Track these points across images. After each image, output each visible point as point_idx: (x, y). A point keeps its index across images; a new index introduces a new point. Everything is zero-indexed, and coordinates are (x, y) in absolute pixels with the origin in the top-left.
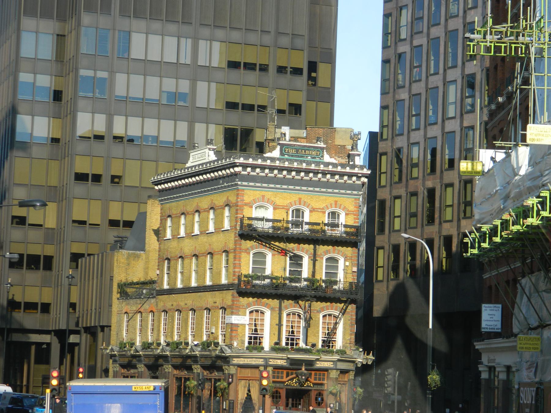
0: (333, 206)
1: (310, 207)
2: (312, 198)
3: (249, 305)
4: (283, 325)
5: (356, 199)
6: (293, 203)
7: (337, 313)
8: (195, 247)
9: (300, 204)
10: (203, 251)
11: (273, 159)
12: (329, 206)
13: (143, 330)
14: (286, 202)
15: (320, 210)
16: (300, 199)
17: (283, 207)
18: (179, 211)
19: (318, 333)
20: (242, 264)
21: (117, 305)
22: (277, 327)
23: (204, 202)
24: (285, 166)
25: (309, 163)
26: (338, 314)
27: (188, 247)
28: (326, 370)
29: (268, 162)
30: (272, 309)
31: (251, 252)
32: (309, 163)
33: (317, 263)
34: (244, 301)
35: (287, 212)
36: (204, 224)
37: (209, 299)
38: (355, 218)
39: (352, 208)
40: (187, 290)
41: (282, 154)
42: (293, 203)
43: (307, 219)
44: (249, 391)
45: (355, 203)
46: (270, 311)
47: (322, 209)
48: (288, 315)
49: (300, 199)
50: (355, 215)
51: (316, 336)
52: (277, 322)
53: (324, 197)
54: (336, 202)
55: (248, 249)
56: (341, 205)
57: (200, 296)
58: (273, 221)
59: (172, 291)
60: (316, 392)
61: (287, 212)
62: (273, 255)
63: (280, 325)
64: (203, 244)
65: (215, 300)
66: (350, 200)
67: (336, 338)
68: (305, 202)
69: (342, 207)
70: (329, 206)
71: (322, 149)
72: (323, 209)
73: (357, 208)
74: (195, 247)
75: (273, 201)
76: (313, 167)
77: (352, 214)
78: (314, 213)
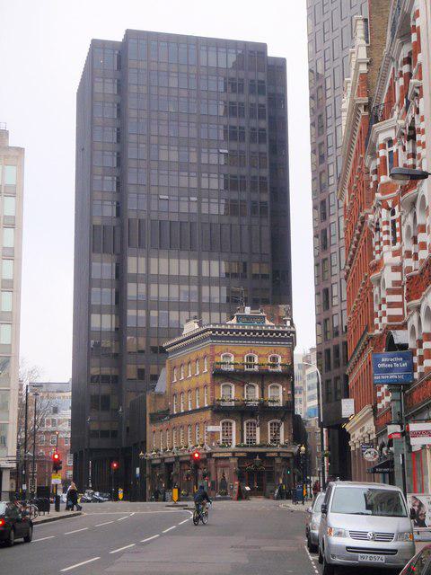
11: (233, 325)
13: (164, 441)
17: (241, 355)
21: (150, 428)
25: (255, 326)
27: (185, 385)
28: (274, 457)
29: (229, 327)
32: (255, 326)
33: (265, 391)
36: (194, 370)
39: (285, 353)
40: (187, 413)
41: (238, 322)
43: (256, 361)
48: (247, 424)
58: (235, 364)
59: (179, 414)
63: (242, 431)
71: (264, 317)
76: (258, 328)
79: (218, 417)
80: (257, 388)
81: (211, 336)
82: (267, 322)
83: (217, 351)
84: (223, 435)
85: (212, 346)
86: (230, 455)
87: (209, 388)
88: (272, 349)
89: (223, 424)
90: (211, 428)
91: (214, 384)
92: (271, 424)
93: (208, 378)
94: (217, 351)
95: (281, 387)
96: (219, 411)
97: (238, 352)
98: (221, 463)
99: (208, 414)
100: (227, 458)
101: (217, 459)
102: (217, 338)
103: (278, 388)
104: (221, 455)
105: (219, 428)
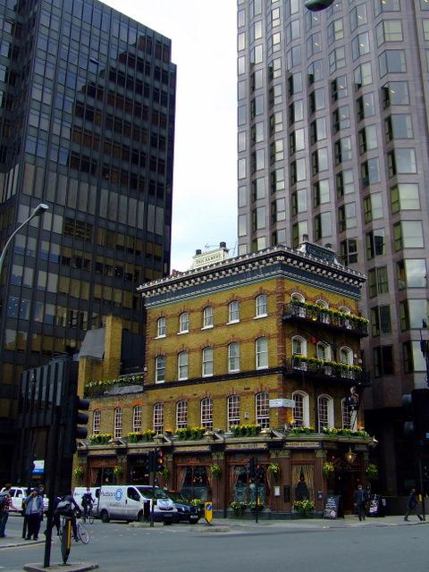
8: (207, 341)
10: (221, 342)
18: (177, 310)
23: (222, 297)
27: (194, 341)
37: (237, 386)
44: (302, 475)
57: (218, 385)
64: (223, 335)
65: (246, 386)
74: (207, 341)
79: (290, 386)
81: (282, 265)
85: (282, 278)
86: (316, 445)
87: (274, 342)
90: (276, 403)
91: (283, 337)
93: (273, 327)
94: (287, 288)
96: (294, 378)
98: (300, 458)
99: (273, 382)
100: (312, 451)
101: (294, 451)
104: (300, 445)
105: (292, 403)
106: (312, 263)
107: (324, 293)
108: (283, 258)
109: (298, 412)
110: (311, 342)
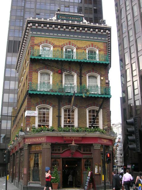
0: (91, 46)
1: (76, 46)
2: (77, 42)
3: (37, 104)
4: (61, 116)
5: (104, 42)
6: (65, 44)
7: (97, 108)
9: (70, 45)
12: (88, 46)
14: (61, 44)
15: (82, 48)
16: (70, 42)
17: (59, 46)
19: (86, 121)
20: (33, 79)
22: (57, 118)
24: (59, 22)
26: (98, 109)
30: (54, 107)
31: (39, 72)
34: (33, 101)
35: (62, 49)
38: (104, 53)
39: (102, 47)
42: (65, 44)
45: (104, 45)
46: (52, 108)
47: (83, 48)
48: (65, 111)
49: (70, 42)
50: (104, 51)
51: (84, 123)
52: (57, 115)
53: (85, 42)
54: (92, 44)
55: (37, 70)
56: (95, 46)
60: (85, 160)
61: (62, 49)
62: (54, 74)
63: (59, 117)
66: (101, 43)
67: (98, 125)
68: (73, 44)
69: (96, 47)
70: (88, 46)
72: (84, 47)
73: (105, 47)
75: (53, 43)
76: (76, 23)
77: (102, 51)
78: (79, 50)
80: (75, 76)
82: (85, 21)
83: (36, 42)
84: (40, 121)
86: (43, 140)
88: (89, 43)
89: (40, 109)
92: (90, 112)
95: (99, 77)
97: (56, 43)
102: (37, 30)
103: (96, 78)
106: (62, 25)
107: (72, 41)
108: (31, 24)
109: (43, 118)
110: (57, 72)
